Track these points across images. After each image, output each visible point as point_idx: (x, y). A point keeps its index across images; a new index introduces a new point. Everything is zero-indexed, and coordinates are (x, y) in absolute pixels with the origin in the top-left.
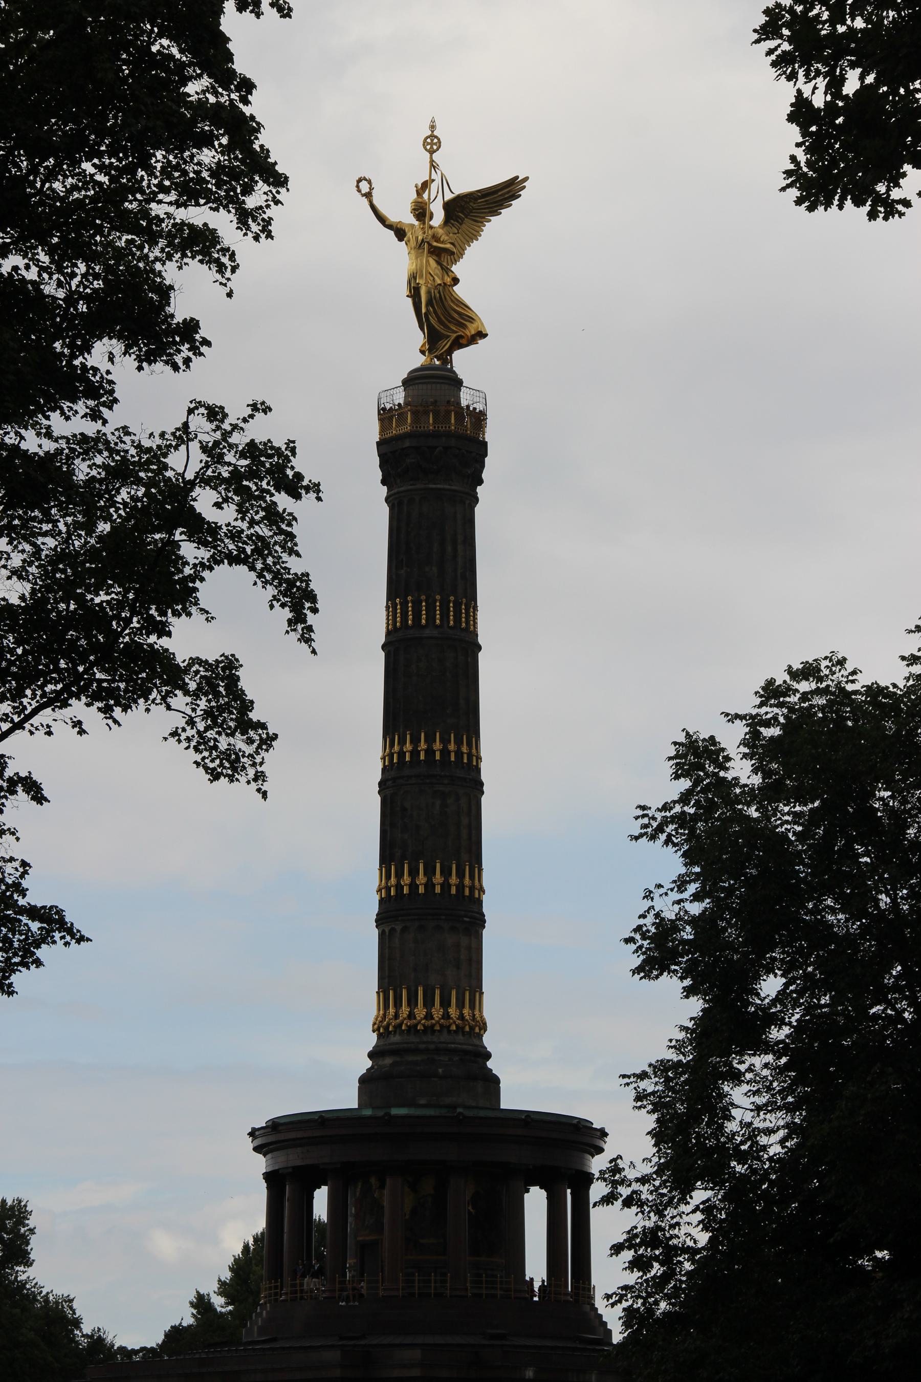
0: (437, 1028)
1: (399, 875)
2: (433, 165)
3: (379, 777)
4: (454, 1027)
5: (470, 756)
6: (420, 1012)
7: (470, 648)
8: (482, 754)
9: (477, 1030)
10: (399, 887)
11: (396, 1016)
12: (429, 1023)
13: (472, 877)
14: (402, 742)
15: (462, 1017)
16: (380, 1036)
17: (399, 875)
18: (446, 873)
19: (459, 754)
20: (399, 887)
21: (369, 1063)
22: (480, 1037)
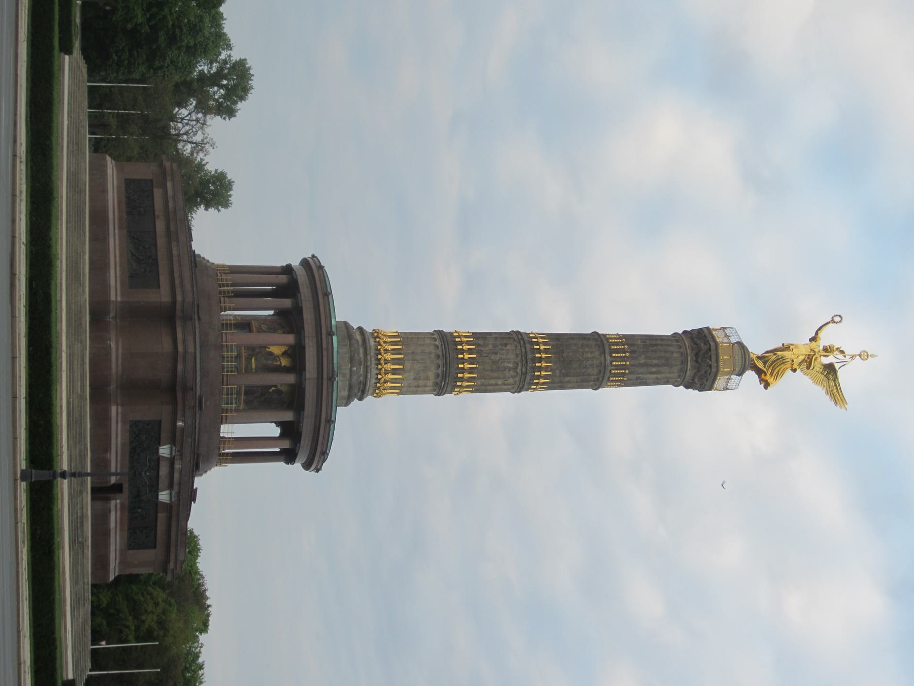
0: (380, 367)
1: (468, 343)
2: (853, 357)
3: (522, 331)
4: (380, 377)
5: (537, 384)
6: (389, 357)
7: (597, 384)
8: (536, 392)
10: (461, 343)
11: (385, 342)
12: (382, 362)
13: (468, 386)
14: (545, 344)
15: (386, 382)
16: (372, 334)
17: (468, 343)
18: (471, 371)
19: (539, 377)
20: (461, 343)
22: (372, 394)
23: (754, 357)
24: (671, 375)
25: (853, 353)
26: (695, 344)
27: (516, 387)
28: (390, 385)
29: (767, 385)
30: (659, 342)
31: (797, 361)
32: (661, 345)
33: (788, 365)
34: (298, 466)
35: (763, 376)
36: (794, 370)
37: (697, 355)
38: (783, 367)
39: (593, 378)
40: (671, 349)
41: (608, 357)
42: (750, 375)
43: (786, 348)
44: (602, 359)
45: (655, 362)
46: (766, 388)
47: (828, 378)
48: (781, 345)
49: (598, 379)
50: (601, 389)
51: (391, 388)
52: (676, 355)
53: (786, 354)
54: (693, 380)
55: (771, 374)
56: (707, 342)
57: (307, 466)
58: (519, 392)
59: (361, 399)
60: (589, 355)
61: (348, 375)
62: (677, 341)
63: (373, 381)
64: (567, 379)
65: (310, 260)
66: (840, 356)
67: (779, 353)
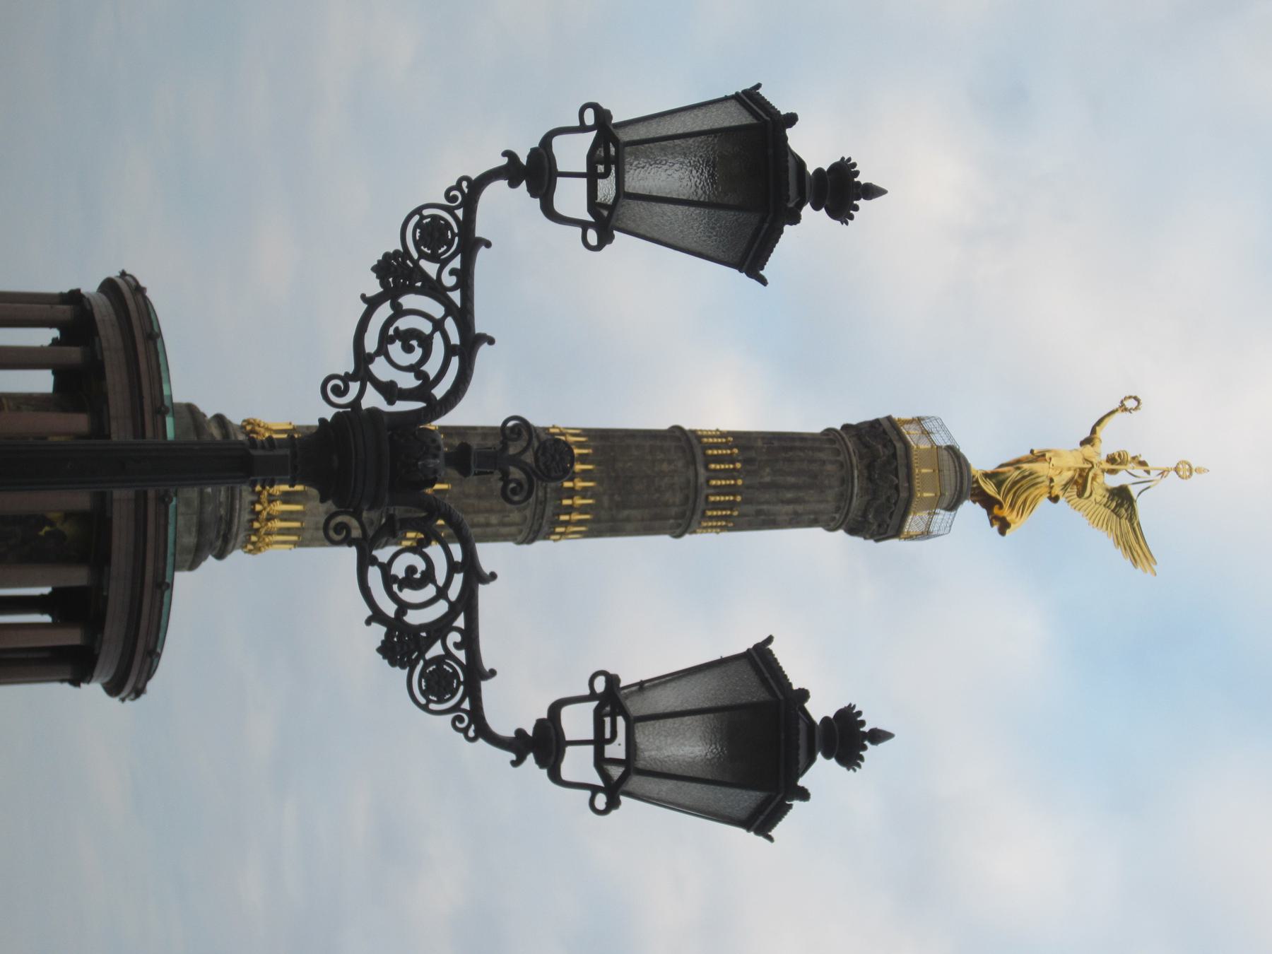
2: (1163, 473)
7: (681, 525)
9: (250, 547)
15: (269, 533)
21: (210, 415)
22: (243, 547)
23: (978, 475)
24: (822, 506)
25: (1164, 466)
26: (866, 445)
27: (524, 534)
28: (278, 524)
29: (1004, 526)
30: (797, 444)
31: (1059, 481)
32: (801, 449)
33: (1043, 489)
34: (93, 690)
35: (996, 510)
36: (1055, 499)
37: (870, 467)
38: (1034, 492)
39: (674, 511)
40: (822, 455)
41: (702, 471)
42: (971, 511)
43: (1039, 457)
44: (691, 474)
45: (792, 480)
46: (1002, 531)
47: (1118, 516)
48: (1027, 453)
49: (683, 515)
50: (687, 537)
51: (282, 531)
52: (829, 467)
53: (1037, 467)
54: (864, 515)
55: (1012, 506)
56: (888, 443)
57: (113, 689)
58: (529, 540)
59: (220, 556)
60: (665, 467)
61: (196, 503)
62: (832, 441)
63: (246, 516)
64: (626, 513)
65: (120, 281)
66: (1139, 471)
67: (1025, 466)
